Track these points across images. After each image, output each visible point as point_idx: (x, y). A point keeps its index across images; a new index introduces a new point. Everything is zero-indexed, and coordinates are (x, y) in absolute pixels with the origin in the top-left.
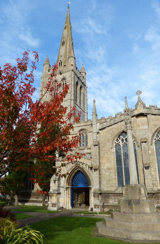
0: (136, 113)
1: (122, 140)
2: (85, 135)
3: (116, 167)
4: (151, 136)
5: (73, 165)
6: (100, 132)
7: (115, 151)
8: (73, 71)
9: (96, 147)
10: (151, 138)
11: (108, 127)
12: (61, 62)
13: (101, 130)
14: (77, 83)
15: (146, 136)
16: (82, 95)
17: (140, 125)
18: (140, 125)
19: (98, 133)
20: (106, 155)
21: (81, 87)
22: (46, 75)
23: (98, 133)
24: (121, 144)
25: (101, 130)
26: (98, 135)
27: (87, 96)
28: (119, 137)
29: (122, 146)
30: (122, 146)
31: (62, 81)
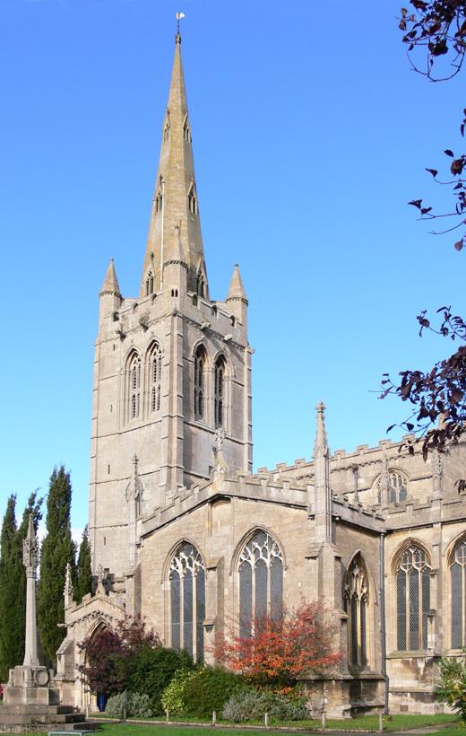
0: (211, 492)
1: (183, 562)
2: (398, 490)
3: (169, 624)
4: (231, 549)
5: (94, 621)
6: (144, 542)
7: (169, 588)
8: (175, 315)
9: (130, 579)
10: (230, 559)
11: (168, 523)
12: (152, 280)
13: (144, 537)
14: (201, 351)
15: (223, 553)
16: (228, 387)
17: (219, 524)
18: (219, 524)
19: (138, 546)
20: (152, 598)
21: (220, 361)
22: (106, 335)
23: (138, 546)
24: (181, 571)
25: (144, 537)
26: (139, 551)
27: (249, 386)
28: (177, 555)
29: (182, 576)
30: (182, 576)
31: (149, 353)
